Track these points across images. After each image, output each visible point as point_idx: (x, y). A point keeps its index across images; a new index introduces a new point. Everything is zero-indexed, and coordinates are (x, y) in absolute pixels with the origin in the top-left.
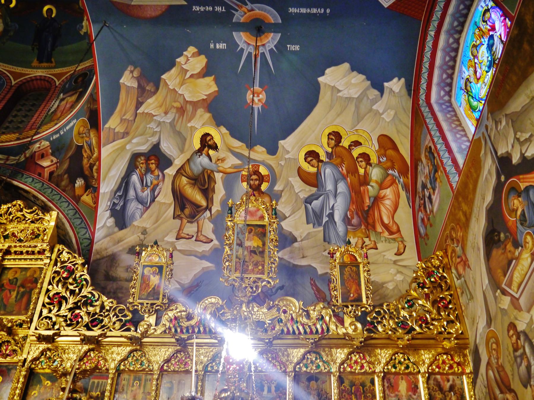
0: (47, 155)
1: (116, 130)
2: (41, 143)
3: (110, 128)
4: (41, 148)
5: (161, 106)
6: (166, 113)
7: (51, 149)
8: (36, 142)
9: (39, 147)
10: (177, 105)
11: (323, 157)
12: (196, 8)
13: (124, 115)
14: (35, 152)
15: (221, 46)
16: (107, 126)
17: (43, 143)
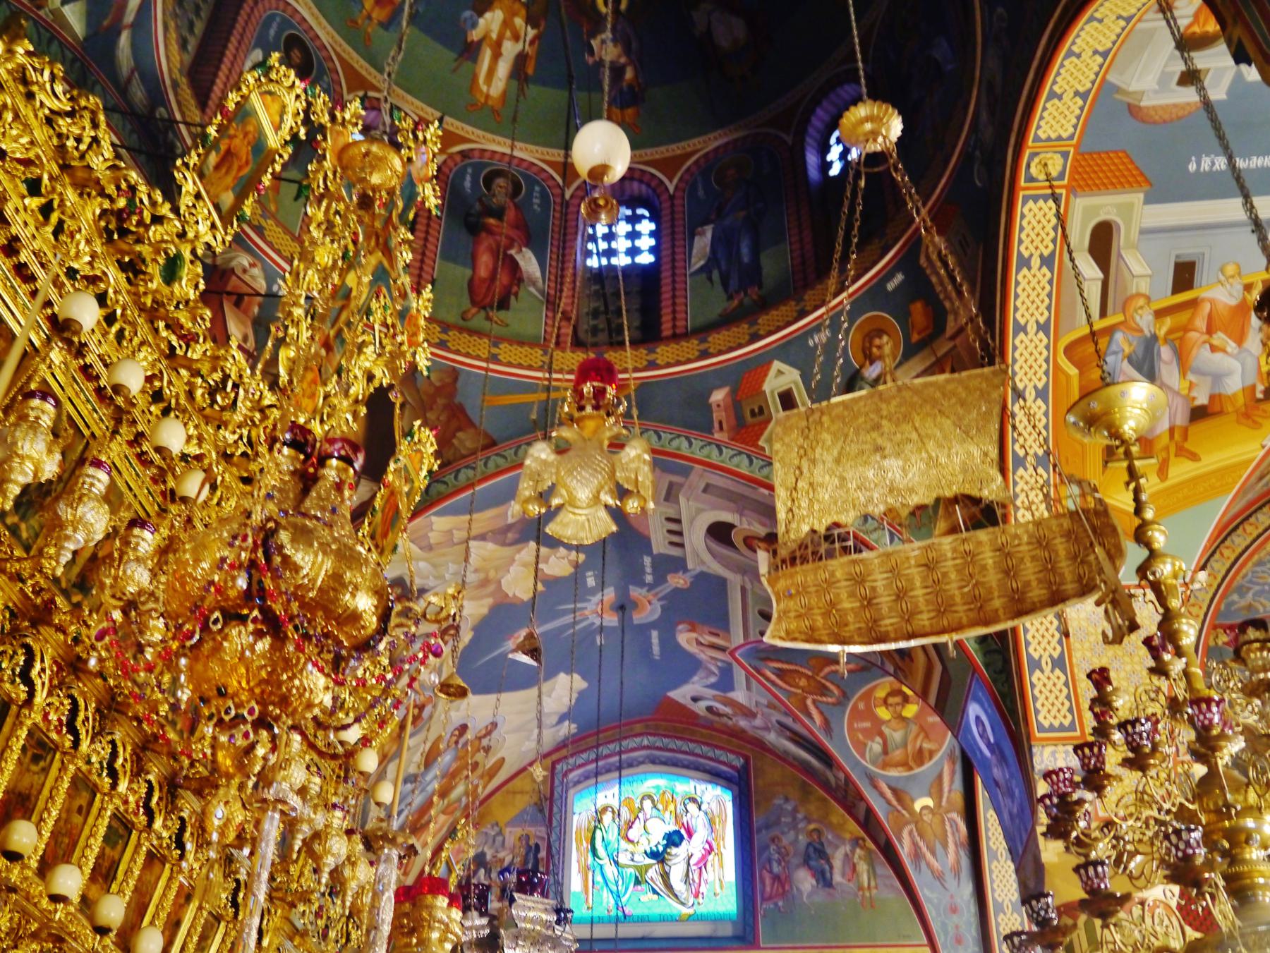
0: (246, 312)
1: (430, 534)
2: (252, 265)
3: (432, 524)
4: (246, 278)
5: (484, 560)
6: (476, 571)
7: (260, 306)
8: (249, 250)
9: (245, 271)
10: (492, 574)
11: (462, 741)
12: (647, 560)
13: (458, 529)
14: (232, 270)
15: (591, 582)
16: (434, 519)
17: (256, 271)
